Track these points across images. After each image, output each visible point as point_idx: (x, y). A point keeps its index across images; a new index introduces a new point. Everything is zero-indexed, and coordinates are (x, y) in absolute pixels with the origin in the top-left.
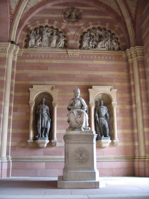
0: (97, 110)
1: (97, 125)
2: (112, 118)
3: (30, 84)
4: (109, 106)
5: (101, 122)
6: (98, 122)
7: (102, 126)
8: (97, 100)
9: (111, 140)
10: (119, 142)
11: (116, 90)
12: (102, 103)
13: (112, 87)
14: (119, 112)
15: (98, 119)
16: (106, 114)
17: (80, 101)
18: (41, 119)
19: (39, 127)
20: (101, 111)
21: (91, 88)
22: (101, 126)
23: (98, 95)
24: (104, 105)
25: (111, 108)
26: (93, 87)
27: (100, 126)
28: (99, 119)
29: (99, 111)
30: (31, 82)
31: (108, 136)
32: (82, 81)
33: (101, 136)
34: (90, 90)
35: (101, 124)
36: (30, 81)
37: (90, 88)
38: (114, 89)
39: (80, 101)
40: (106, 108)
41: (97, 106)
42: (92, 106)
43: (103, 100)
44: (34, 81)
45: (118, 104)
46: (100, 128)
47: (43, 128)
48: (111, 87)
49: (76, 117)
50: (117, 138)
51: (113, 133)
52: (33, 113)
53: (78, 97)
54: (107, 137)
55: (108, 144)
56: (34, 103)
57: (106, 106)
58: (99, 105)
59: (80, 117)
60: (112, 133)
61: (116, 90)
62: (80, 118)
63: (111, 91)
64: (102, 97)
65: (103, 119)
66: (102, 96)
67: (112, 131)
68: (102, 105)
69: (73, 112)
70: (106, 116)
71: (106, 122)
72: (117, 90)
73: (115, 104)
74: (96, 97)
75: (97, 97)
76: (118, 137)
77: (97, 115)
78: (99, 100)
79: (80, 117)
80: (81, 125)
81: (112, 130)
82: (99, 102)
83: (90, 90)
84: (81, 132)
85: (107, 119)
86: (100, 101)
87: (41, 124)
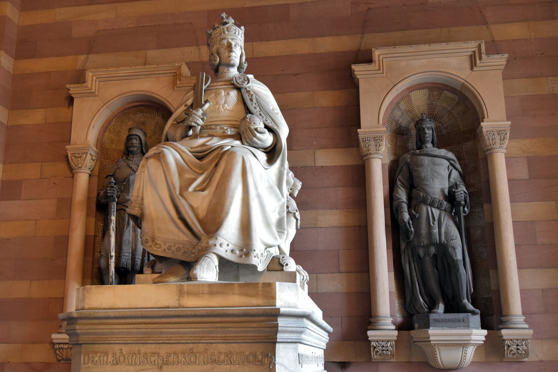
0: (405, 168)
1: (403, 246)
2: (486, 206)
3: (79, 66)
4: (468, 145)
5: (424, 230)
6: (407, 232)
7: (433, 250)
8: (404, 121)
9: (483, 327)
10: (535, 337)
11: (500, 60)
12: (429, 132)
13: (479, 46)
14: (523, 173)
15: (406, 216)
16: (450, 188)
17: (239, 89)
18: (113, 225)
19: (108, 265)
20: (423, 175)
21: (370, 61)
22: (427, 254)
23: (406, 95)
24: (440, 143)
25: (481, 156)
26: (377, 53)
27: (421, 253)
28: (412, 217)
29: (414, 174)
30: (82, 57)
31: (470, 307)
32: (322, 35)
33: (432, 306)
34: (358, 69)
35: (425, 241)
36: (81, 54)
37: (357, 62)
38: (488, 54)
39: (234, 94)
40: (451, 155)
41: (406, 150)
42: (372, 149)
43: (433, 117)
44: (97, 53)
45: (515, 133)
46: (419, 260)
47: (126, 269)
48: (472, 46)
49: (177, 186)
50: (522, 319)
51: (498, 292)
52: (89, 198)
53: (234, 72)
54: (464, 310)
55: (470, 351)
56: (93, 150)
57: (451, 150)
58: (412, 144)
59: (202, 188)
60: (493, 288)
61: (500, 60)
62: (206, 192)
63: (473, 64)
64: (431, 106)
65: (436, 212)
66: (429, 98)
67: (493, 281)
68: (429, 145)
69: (160, 157)
70: (451, 197)
71: (455, 232)
72: (508, 61)
73: (499, 132)
74: (395, 104)
75: (403, 106)
76: (524, 314)
77: (402, 195)
78: (413, 119)
79: (202, 188)
80: (203, 244)
81: (492, 272)
82: (414, 132)
83: (358, 69)
84: (181, 293)
85: (457, 214)
86: (419, 124)
87: (113, 254)
